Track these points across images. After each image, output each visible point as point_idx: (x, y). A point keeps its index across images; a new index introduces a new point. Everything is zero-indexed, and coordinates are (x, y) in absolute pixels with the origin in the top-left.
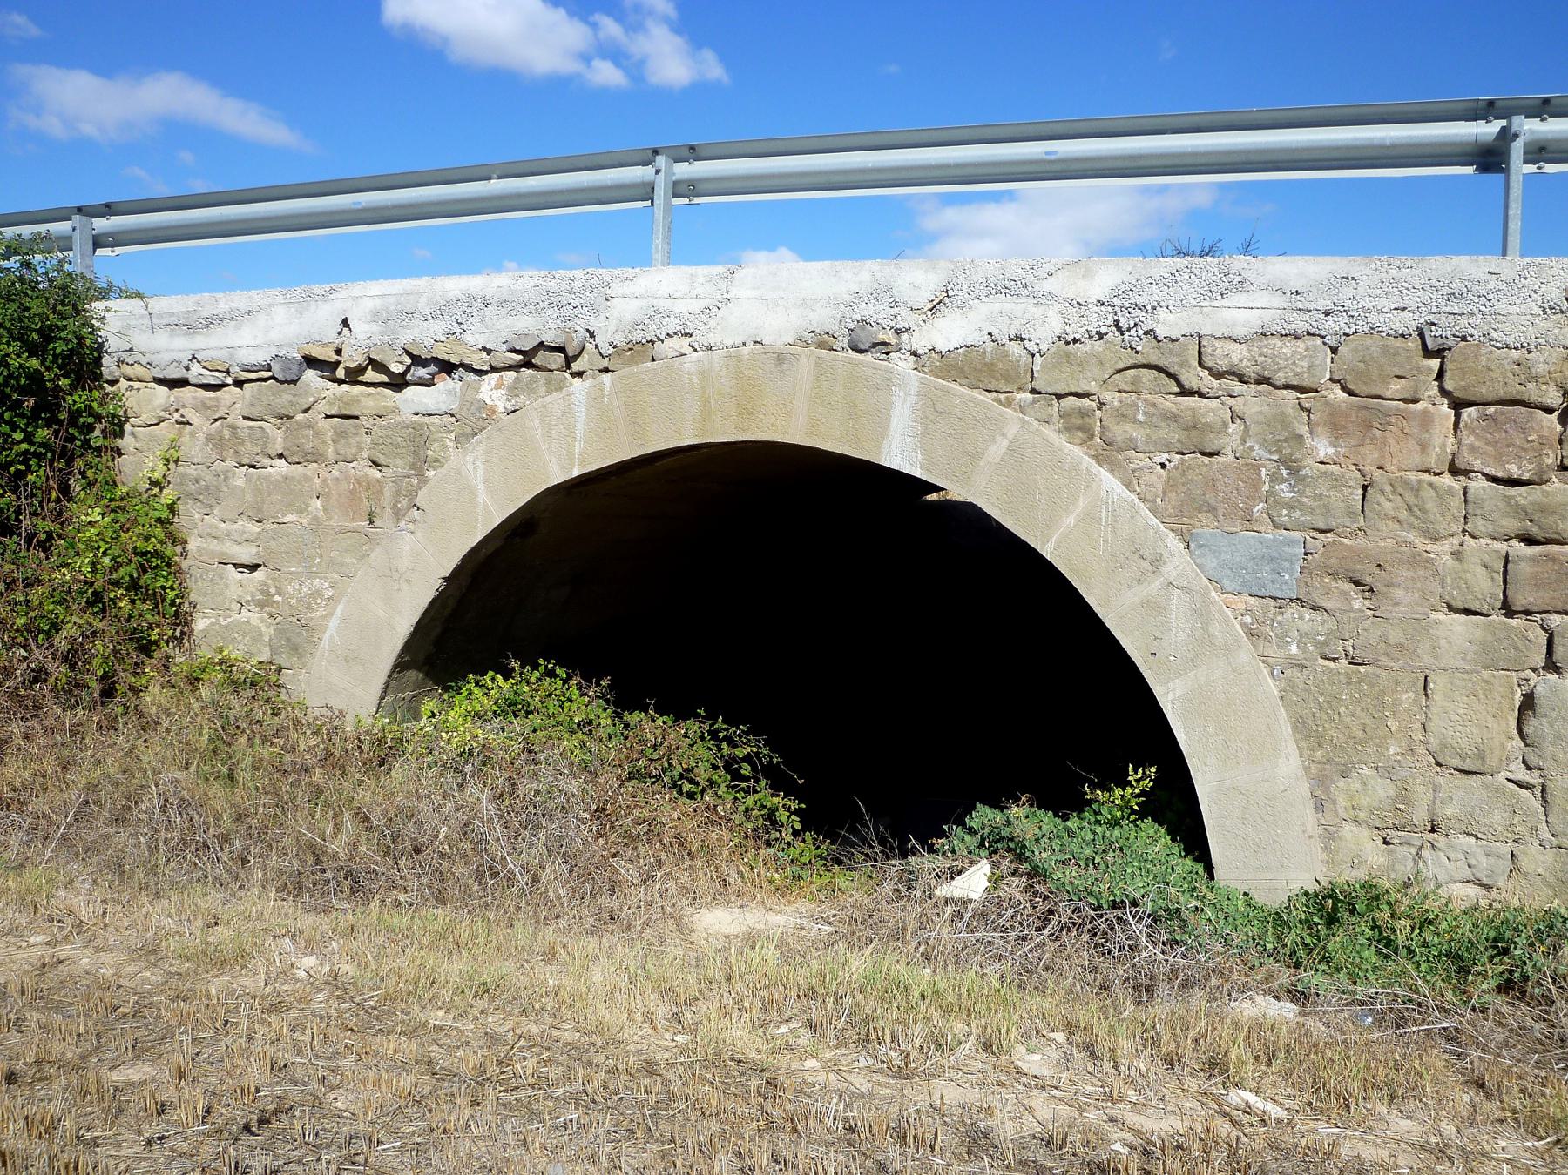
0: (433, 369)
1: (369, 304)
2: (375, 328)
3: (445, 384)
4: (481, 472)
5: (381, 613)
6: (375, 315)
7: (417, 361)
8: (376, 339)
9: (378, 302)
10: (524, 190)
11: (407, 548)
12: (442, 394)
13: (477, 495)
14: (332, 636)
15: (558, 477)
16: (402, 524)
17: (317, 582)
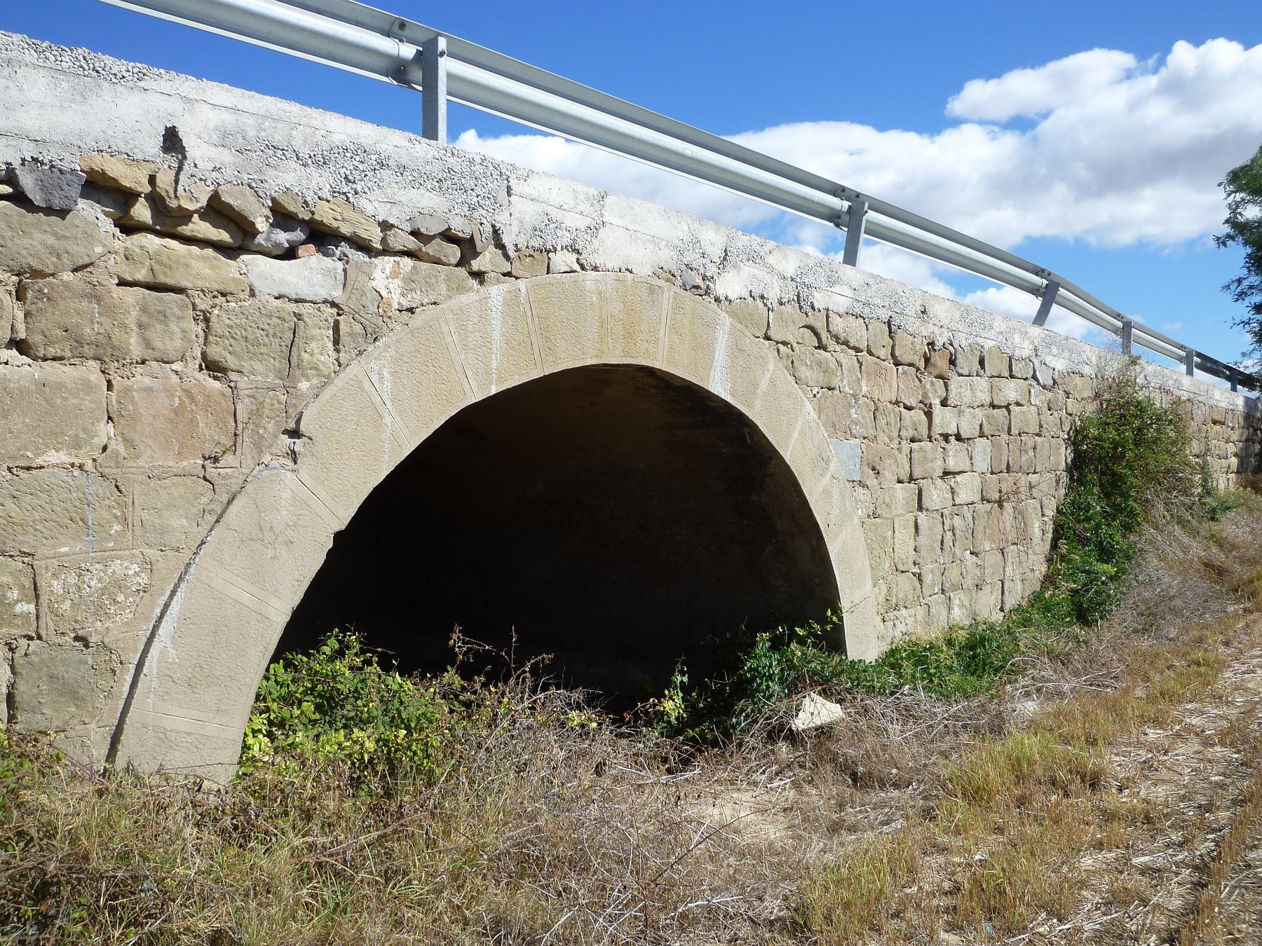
0: (299, 235)
1: (213, 118)
2: (225, 157)
3: (312, 263)
4: (387, 386)
5: (246, 598)
6: (224, 138)
7: (283, 218)
8: (230, 173)
9: (228, 119)
10: (781, 186)
11: (287, 494)
12: (312, 273)
13: (377, 419)
14: (164, 651)
15: (476, 395)
16: (267, 458)
17: (116, 567)
